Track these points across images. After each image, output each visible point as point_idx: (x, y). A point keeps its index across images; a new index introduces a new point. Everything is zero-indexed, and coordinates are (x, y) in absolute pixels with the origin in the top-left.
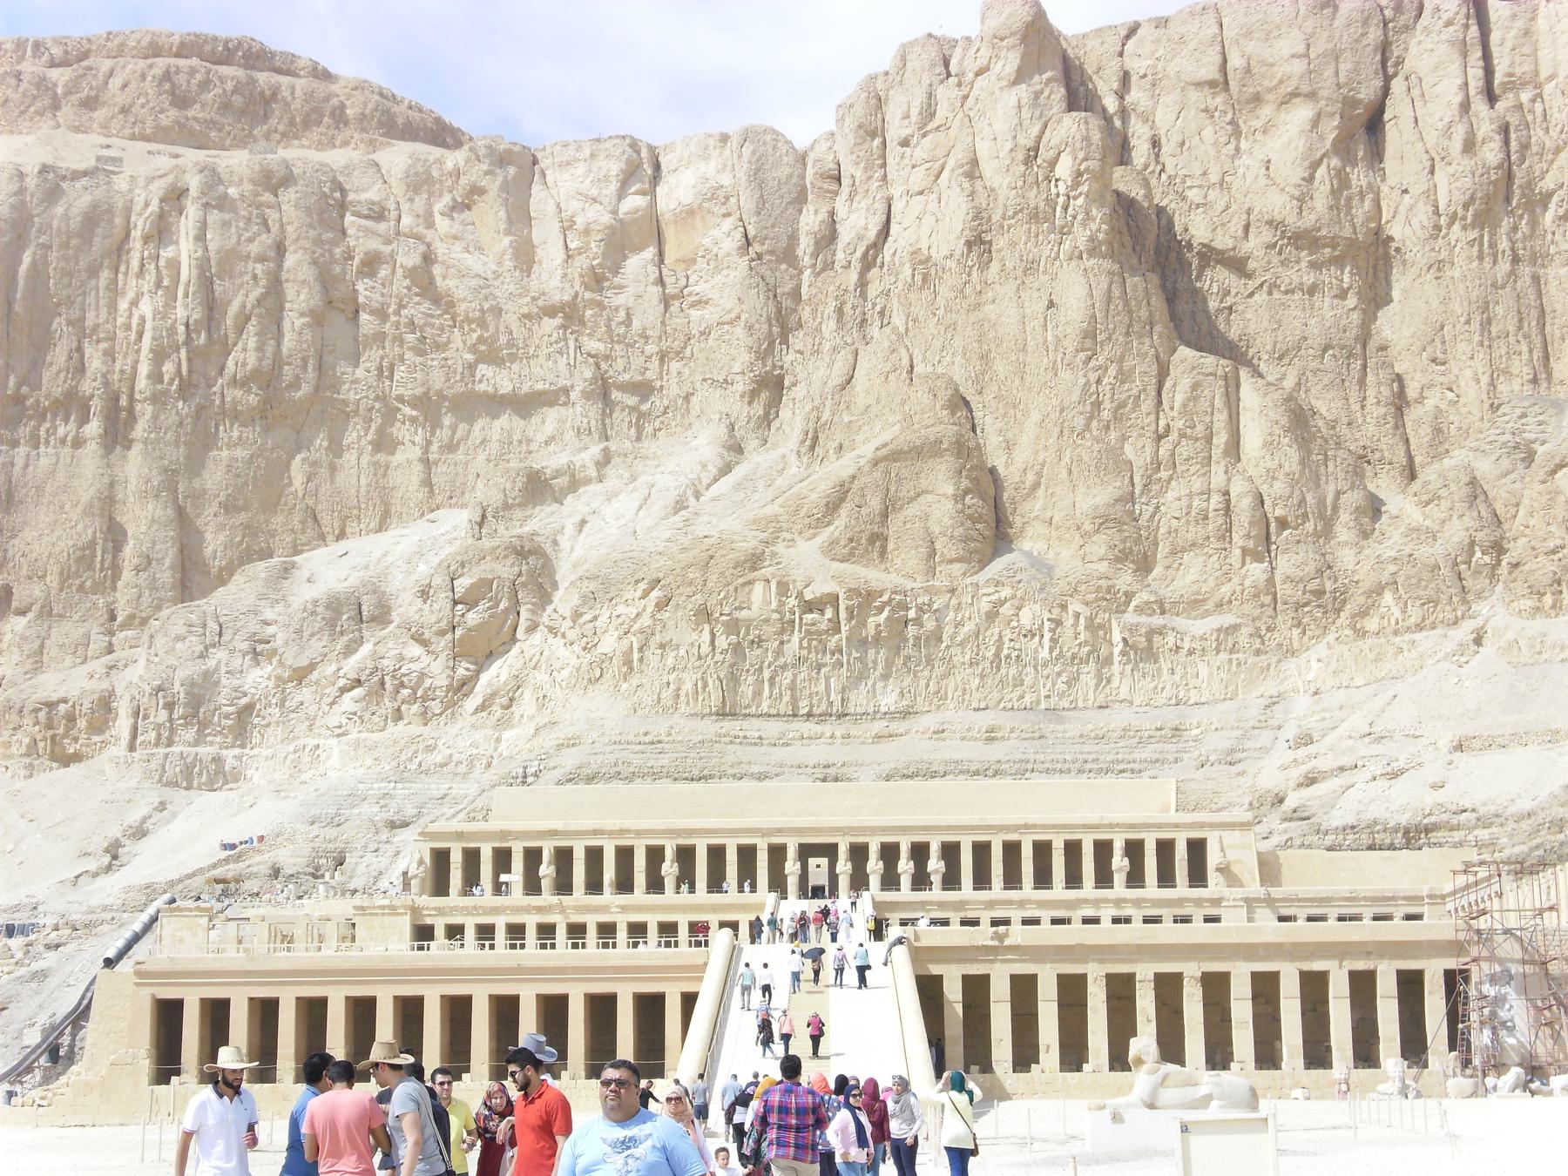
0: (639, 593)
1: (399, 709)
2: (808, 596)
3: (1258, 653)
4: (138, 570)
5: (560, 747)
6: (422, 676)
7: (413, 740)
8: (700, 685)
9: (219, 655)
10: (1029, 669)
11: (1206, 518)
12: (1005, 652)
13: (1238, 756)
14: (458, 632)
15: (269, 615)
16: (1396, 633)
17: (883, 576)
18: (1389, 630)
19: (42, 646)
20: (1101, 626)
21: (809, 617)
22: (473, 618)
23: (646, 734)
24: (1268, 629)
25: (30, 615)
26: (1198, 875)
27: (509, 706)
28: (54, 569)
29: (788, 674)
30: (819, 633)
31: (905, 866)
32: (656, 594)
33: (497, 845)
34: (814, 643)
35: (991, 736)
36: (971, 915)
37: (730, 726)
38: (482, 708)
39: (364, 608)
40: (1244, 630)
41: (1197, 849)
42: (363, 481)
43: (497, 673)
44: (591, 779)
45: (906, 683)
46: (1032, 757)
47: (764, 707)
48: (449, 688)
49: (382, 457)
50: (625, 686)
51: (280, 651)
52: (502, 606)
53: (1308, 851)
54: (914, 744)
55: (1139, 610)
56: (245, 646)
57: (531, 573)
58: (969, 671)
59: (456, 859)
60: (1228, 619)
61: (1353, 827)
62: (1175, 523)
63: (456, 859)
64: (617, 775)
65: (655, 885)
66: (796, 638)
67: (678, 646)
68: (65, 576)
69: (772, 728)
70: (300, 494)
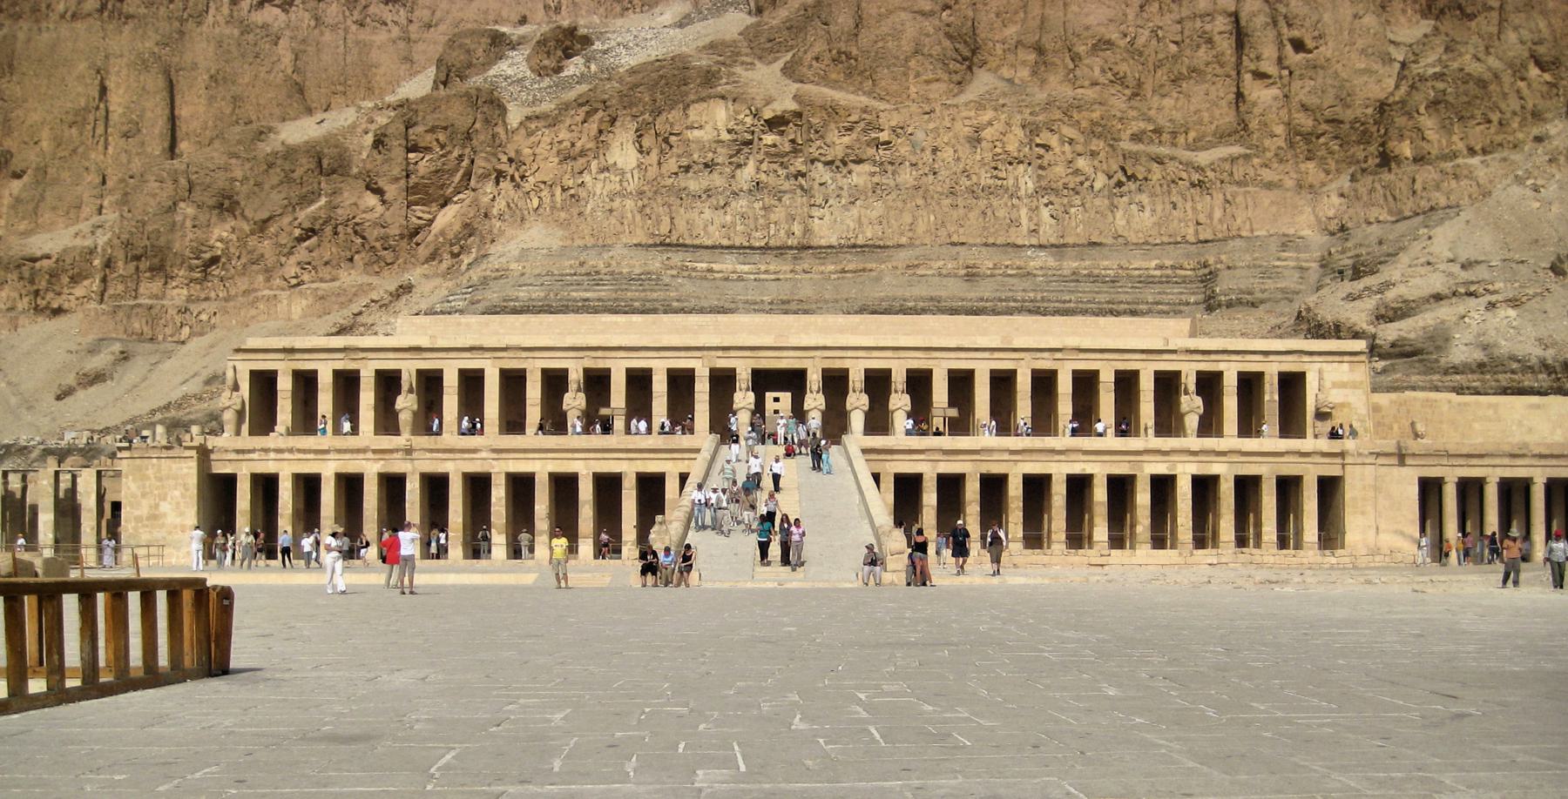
0: (579, 119)
1: (351, 260)
2: (768, 114)
3: (1269, 186)
4: (126, 136)
5: (485, 281)
6: (375, 224)
7: (362, 289)
8: (648, 211)
9: (187, 209)
10: (1015, 201)
11: (1210, 41)
12: (991, 182)
13: (1259, 295)
14: (413, 180)
15: (238, 174)
16: (1445, 157)
17: (852, 97)
18: (1434, 152)
19: (37, 207)
20: (1093, 154)
21: (769, 139)
22: (424, 165)
23: (582, 264)
24: (1281, 161)
25: (25, 178)
26: (1291, 424)
27: (458, 255)
28: (45, 134)
29: (741, 204)
30: (776, 155)
31: (900, 402)
32: (600, 114)
33: (340, 365)
34: (775, 166)
35: (971, 276)
36: (996, 469)
37: (677, 258)
38: (433, 256)
39: (325, 162)
40: (1256, 161)
41: (1292, 384)
42: (349, 59)
43: (447, 218)
44: (515, 311)
45: (875, 214)
46: (1019, 296)
47: (716, 237)
48: (402, 236)
49: (364, 35)
50: (563, 215)
51: (243, 203)
52: (456, 154)
53: (1433, 395)
54: (889, 281)
55: (1136, 138)
56: (211, 202)
57: (487, 121)
58: (947, 202)
59: (285, 384)
60: (1236, 150)
61: (1481, 365)
62: (1173, 48)
63: (285, 384)
64: (549, 310)
65: (555, 421)
66: (751, 164)
67: (623, 174)
68: (58, 142)
69: (727, 264)
70: (289, 71)
